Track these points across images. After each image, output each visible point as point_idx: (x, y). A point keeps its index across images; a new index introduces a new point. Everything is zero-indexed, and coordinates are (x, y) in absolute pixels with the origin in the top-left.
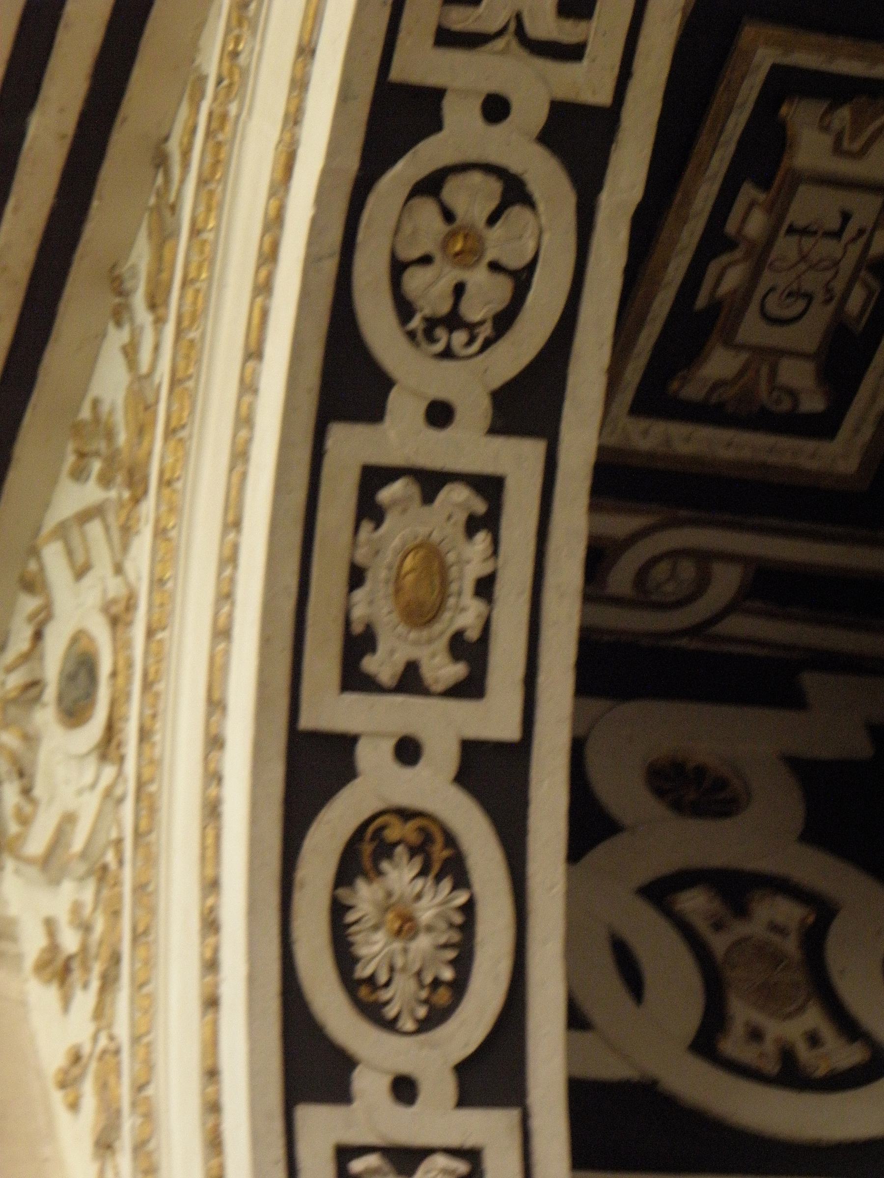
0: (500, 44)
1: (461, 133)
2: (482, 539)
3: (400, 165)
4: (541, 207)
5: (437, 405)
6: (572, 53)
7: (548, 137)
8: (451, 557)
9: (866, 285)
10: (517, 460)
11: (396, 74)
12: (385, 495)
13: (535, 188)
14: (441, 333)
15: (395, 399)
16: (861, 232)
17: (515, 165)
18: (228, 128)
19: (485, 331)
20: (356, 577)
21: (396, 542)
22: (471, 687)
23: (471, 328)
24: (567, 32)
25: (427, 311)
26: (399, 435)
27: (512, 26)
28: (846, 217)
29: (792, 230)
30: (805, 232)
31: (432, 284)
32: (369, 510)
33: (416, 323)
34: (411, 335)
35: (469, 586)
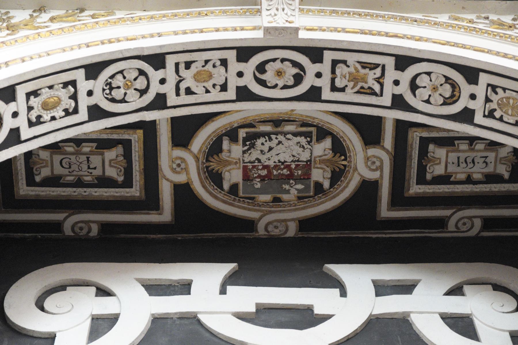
0: (177, 77)
1: (155, 75)
2: (63, 114)
3: (146, 64)
4: (141, 99)
5: (92, 91)
6: (178, 94)
7: (158, 95)
8: (58, 108)
9: (74, 179)
10: (83, 115)
11: (167, 56)
12: (70, 87)
13: (145, 97)
14: (108, 87)
15: (92, 81)
16: (91, 173)
17: (150, 90)
18: (124, 23)
19: (110, 97)
20: (51, 87)
21: (60, 94)
22: (31, 124)
23: (110, 93)
24: (182, 91)
25: (113, 82)
26: (84, 86)
27: (181, 79)
28: (95, 168)
29: (88, 158)
30: (88, 161)
31: (119, 81)
32: (65, 85)
33: (110, 80)
34: (107, 80)
35: (52, 115)
